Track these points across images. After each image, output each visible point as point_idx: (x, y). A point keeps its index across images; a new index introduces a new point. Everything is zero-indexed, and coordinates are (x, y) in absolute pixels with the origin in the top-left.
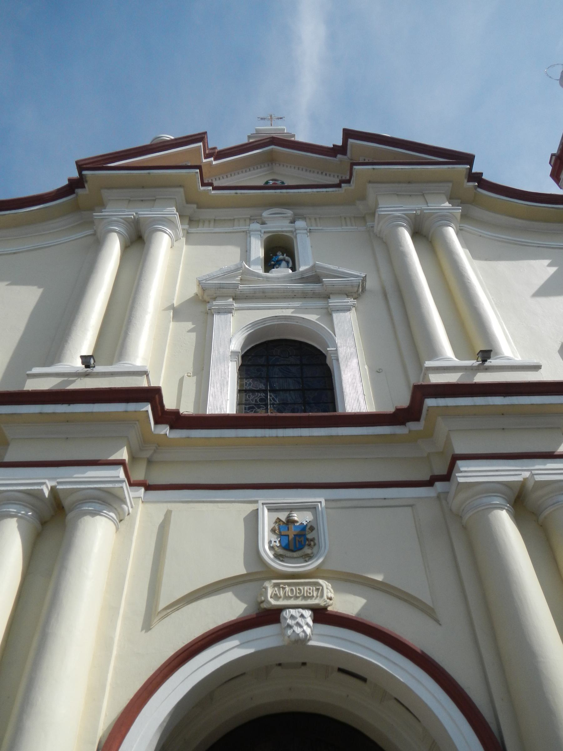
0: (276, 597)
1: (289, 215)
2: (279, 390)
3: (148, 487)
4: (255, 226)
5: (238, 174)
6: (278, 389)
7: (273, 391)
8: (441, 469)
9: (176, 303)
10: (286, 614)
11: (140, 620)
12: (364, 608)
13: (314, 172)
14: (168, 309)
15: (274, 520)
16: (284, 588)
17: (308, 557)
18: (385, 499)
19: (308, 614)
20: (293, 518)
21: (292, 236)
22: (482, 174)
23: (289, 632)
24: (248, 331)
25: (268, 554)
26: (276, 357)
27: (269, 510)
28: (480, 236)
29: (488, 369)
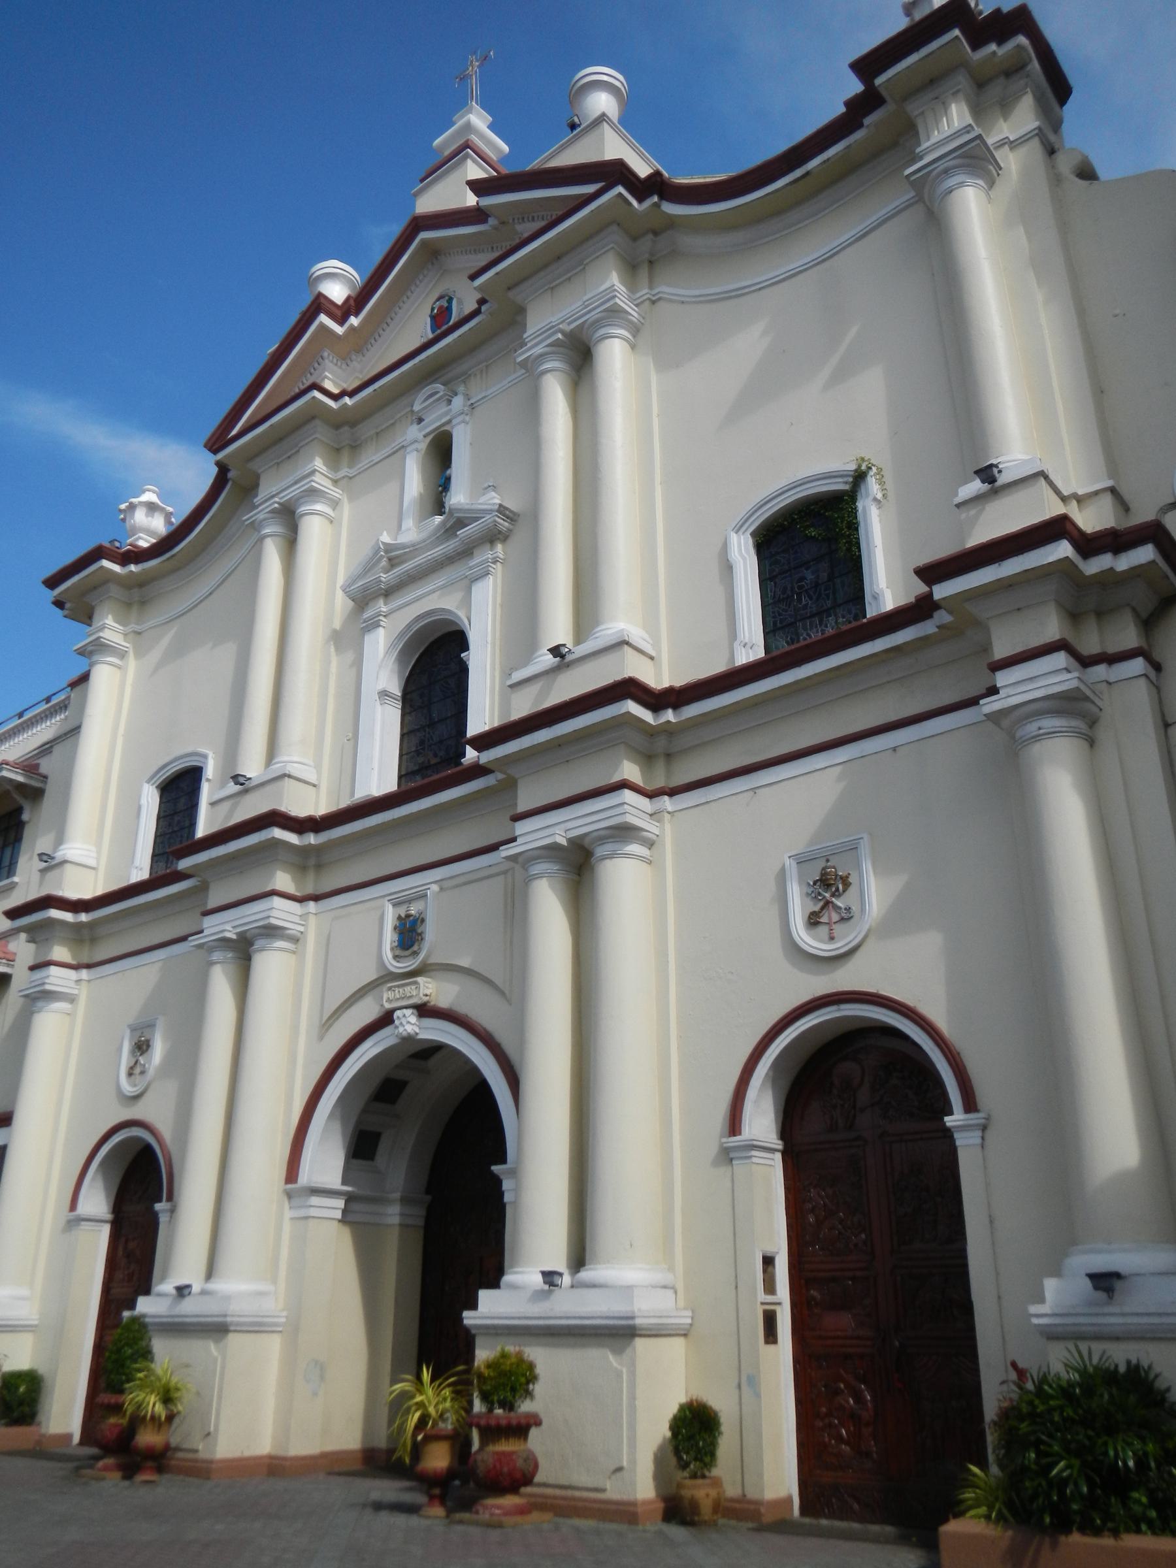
0: (389, 1000)
1: (441, 394)
3: (316, 898)
6: (436, 720)
9: (337, 624)
13: (483, 251)
15: (397, 916)
16: (394, 991)
17: (416, 954)
18: (490, 866)
20: (410, 912)
23: (397, 1031)
24: (396, 650)
26: (440, 666)
27: (394, 905)
28: (683, 302)
29: (568, 665)
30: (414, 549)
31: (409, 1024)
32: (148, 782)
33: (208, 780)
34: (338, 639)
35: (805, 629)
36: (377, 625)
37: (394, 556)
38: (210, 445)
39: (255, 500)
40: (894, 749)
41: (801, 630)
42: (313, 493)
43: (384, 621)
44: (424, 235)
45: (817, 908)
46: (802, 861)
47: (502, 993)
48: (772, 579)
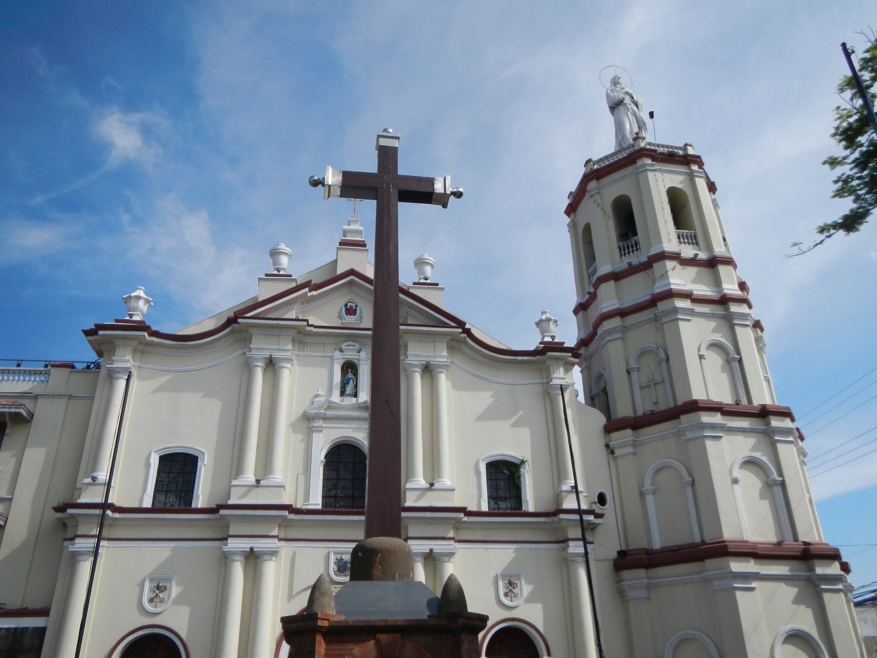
1: (357, 348)
2: (343, 479)
4: (337, 354)
6: (342, 478)
9: (293, 421)
14: (289, 426)
21: (358, 364)
22: (470, 329)
27: (334, 553)
30: (341, 407)
32: (155, 452)
33: (204, 465)
34: (294, 426)
35: (500, 500)
36: (321, 431)
37: (330, 406)
38: (237, 314)
40: (531, 549)
41: (499, 501)
42: (289, 360)
43: (323, 431)
44: (352, 277)
45: (507, 591)
46: (503, 576)
48: (490, 480)
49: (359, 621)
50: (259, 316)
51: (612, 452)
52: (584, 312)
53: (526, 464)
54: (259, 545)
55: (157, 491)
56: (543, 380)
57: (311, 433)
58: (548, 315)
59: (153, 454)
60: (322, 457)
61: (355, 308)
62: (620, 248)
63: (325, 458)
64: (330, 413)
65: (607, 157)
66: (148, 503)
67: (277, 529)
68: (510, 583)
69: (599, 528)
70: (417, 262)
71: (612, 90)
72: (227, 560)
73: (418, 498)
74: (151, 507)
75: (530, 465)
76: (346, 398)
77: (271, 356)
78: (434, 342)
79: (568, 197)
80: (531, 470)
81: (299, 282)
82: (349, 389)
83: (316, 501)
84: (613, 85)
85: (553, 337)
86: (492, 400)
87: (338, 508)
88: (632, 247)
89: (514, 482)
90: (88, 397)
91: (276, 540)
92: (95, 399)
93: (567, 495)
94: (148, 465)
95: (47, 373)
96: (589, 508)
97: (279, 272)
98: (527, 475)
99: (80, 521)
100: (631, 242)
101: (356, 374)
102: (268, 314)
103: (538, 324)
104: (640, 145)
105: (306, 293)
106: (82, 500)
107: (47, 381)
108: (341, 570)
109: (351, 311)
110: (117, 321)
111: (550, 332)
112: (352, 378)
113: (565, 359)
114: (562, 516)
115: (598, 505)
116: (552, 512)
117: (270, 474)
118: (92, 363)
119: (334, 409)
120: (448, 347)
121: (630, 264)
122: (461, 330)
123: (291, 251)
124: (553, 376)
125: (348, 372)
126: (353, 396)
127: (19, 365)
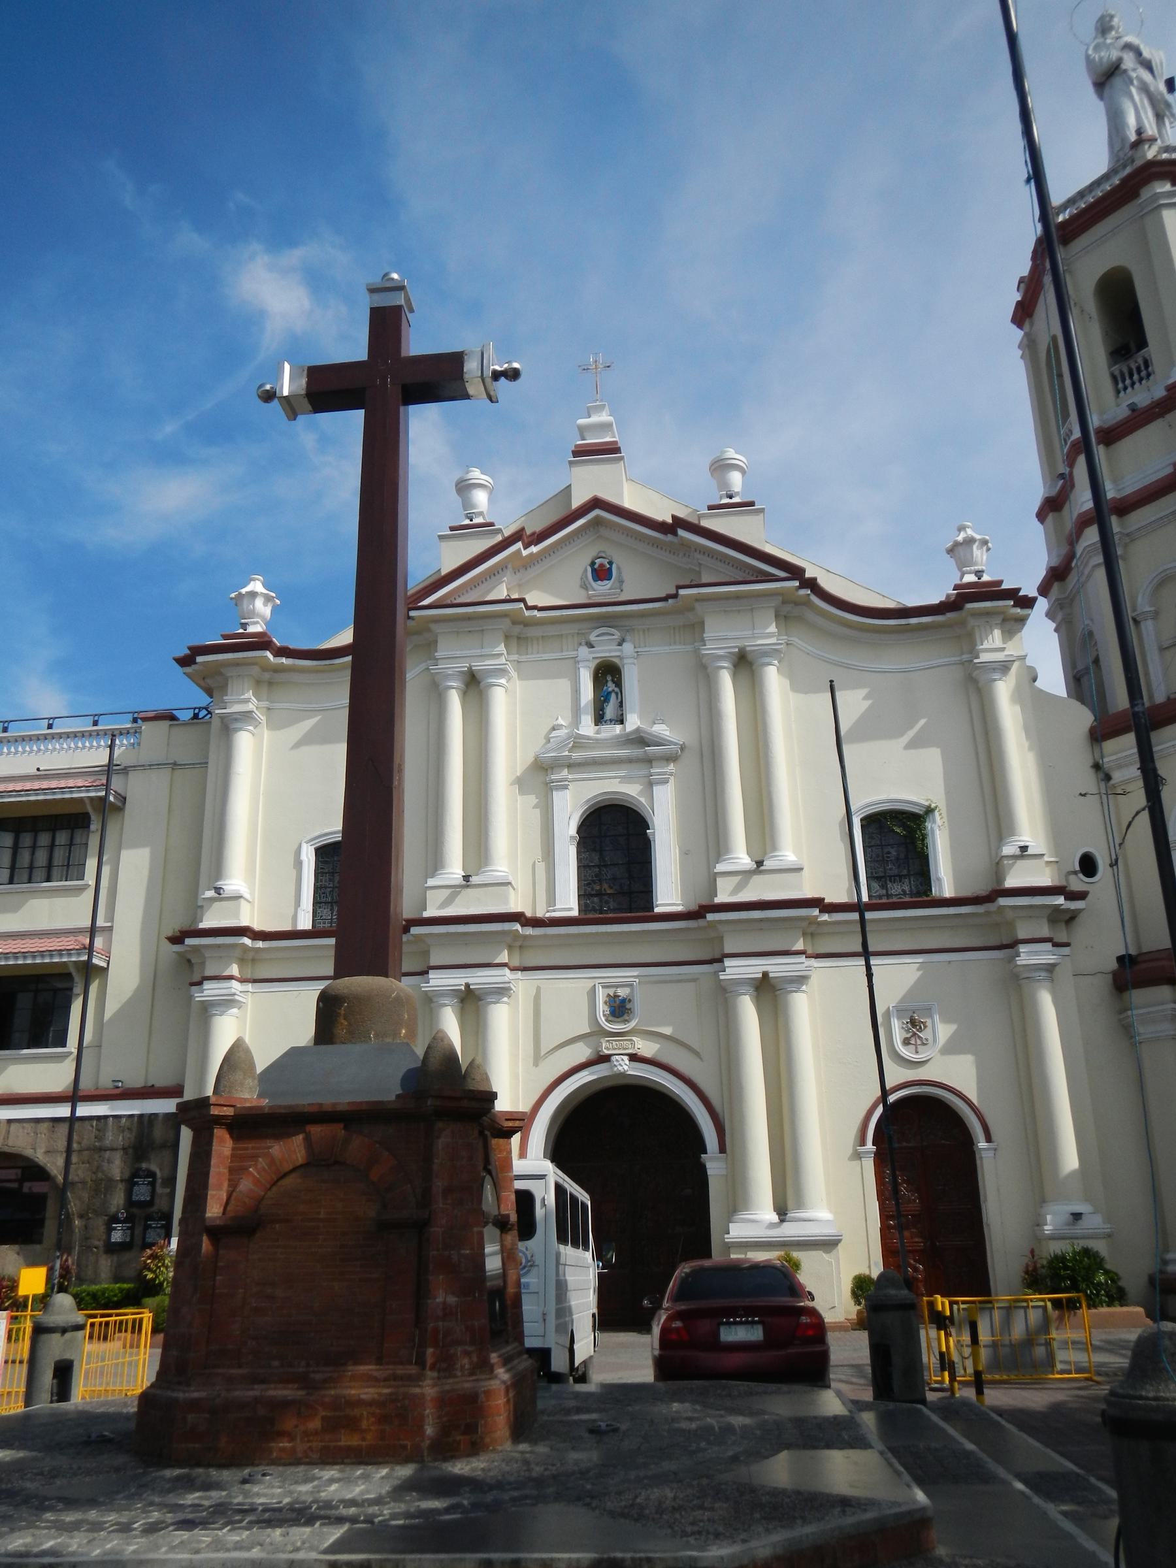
0: (607, 1049)
4: (584, 651)
5: (562, 548)
7: (606, 866)
8: (717, 956)
9: (518, 774)
10: (614, 1058)
11: (531, 1061)
12: (659, 1050)
17: (627, 1021)
19: (626, 1058)
21: (621, 666)
23: (616, 1069)
25: (602, 1020)
30: (597, 743)
31: (623, 1065)
34: (521, 783)
35: (891, 881)
36: (566, 787)
37: (579, 742)
39: (436, 654)
40: (950, 962)
41: (888, 882)
42: (501, 672)
45: (909, 1035)
47: (697, 1054)
48: (870, 847)
49: (280, 1107)
50: (444, 603)
51: (1108, 778)
52: (1056, 514)
53: (937, 813)
54: (479, 979)
55: (317, 903)
56: (964, 656)
57: (550, 793)
58: (969, 531)
59: (304, 846)
60: (573, 830)
61: (608, 566)
62: (1114, 378)
63: (578, 833)
64: (577, 755)
65: (1081, 194)
66: (305, 922)
67: (506, 952)
68: (913, 1022)
69: (1081, 918)
70: (716, 465)
71: (1097, 48)
72: (432, 1005)
73: (738, 889)
74: (310, 927)
75: (944, 814)
76: (603, 727)
77: (470, 668)
78: (752, 610)
79: (1018, 290)
80: (946, 824)
81: (507, 533)
82: (610, 711)
83: (568, 902)
84: (1100, 35)
85: (979, 573)
86: (869, 702)
87: (606, 912)
88: (1139, 370)
89: (915, 847)
90: (199, 764)
91: (507, 971)
92: (210, 765)
93: (1013, 864)
94: (298, 864)
95: (137, 732)
96: (1057, 883)
97: (471, 520)
98: (937, 832)
99: (207, 955)
100: (1136, 362)
101: (619, 684)
102: (459, 596)
103: (950, 551)
104: (1144, 156)
105: (519, 551)
106: (205, 924)
107: (139, 744)
108: (617, 1014)
109: (601, 573)
110: (225, 637)
111: (976, 564)
112: (613, 690)
113: (1003, 613)
114: (1003, 901)
115: (1081, 876)
116: (984, 894)
117: (486, 864)
118: (200, 709)
119: (585, 747)
120: (777, 616)
121: (1133, 408)
122: (797, 583)
123: (491, 481)
124: (981, 647)
125: (607, 681)
126: (617, 721)
127: (95, 723)
